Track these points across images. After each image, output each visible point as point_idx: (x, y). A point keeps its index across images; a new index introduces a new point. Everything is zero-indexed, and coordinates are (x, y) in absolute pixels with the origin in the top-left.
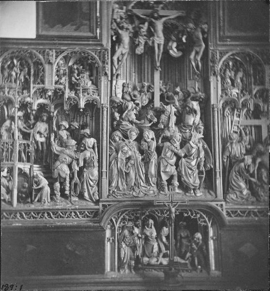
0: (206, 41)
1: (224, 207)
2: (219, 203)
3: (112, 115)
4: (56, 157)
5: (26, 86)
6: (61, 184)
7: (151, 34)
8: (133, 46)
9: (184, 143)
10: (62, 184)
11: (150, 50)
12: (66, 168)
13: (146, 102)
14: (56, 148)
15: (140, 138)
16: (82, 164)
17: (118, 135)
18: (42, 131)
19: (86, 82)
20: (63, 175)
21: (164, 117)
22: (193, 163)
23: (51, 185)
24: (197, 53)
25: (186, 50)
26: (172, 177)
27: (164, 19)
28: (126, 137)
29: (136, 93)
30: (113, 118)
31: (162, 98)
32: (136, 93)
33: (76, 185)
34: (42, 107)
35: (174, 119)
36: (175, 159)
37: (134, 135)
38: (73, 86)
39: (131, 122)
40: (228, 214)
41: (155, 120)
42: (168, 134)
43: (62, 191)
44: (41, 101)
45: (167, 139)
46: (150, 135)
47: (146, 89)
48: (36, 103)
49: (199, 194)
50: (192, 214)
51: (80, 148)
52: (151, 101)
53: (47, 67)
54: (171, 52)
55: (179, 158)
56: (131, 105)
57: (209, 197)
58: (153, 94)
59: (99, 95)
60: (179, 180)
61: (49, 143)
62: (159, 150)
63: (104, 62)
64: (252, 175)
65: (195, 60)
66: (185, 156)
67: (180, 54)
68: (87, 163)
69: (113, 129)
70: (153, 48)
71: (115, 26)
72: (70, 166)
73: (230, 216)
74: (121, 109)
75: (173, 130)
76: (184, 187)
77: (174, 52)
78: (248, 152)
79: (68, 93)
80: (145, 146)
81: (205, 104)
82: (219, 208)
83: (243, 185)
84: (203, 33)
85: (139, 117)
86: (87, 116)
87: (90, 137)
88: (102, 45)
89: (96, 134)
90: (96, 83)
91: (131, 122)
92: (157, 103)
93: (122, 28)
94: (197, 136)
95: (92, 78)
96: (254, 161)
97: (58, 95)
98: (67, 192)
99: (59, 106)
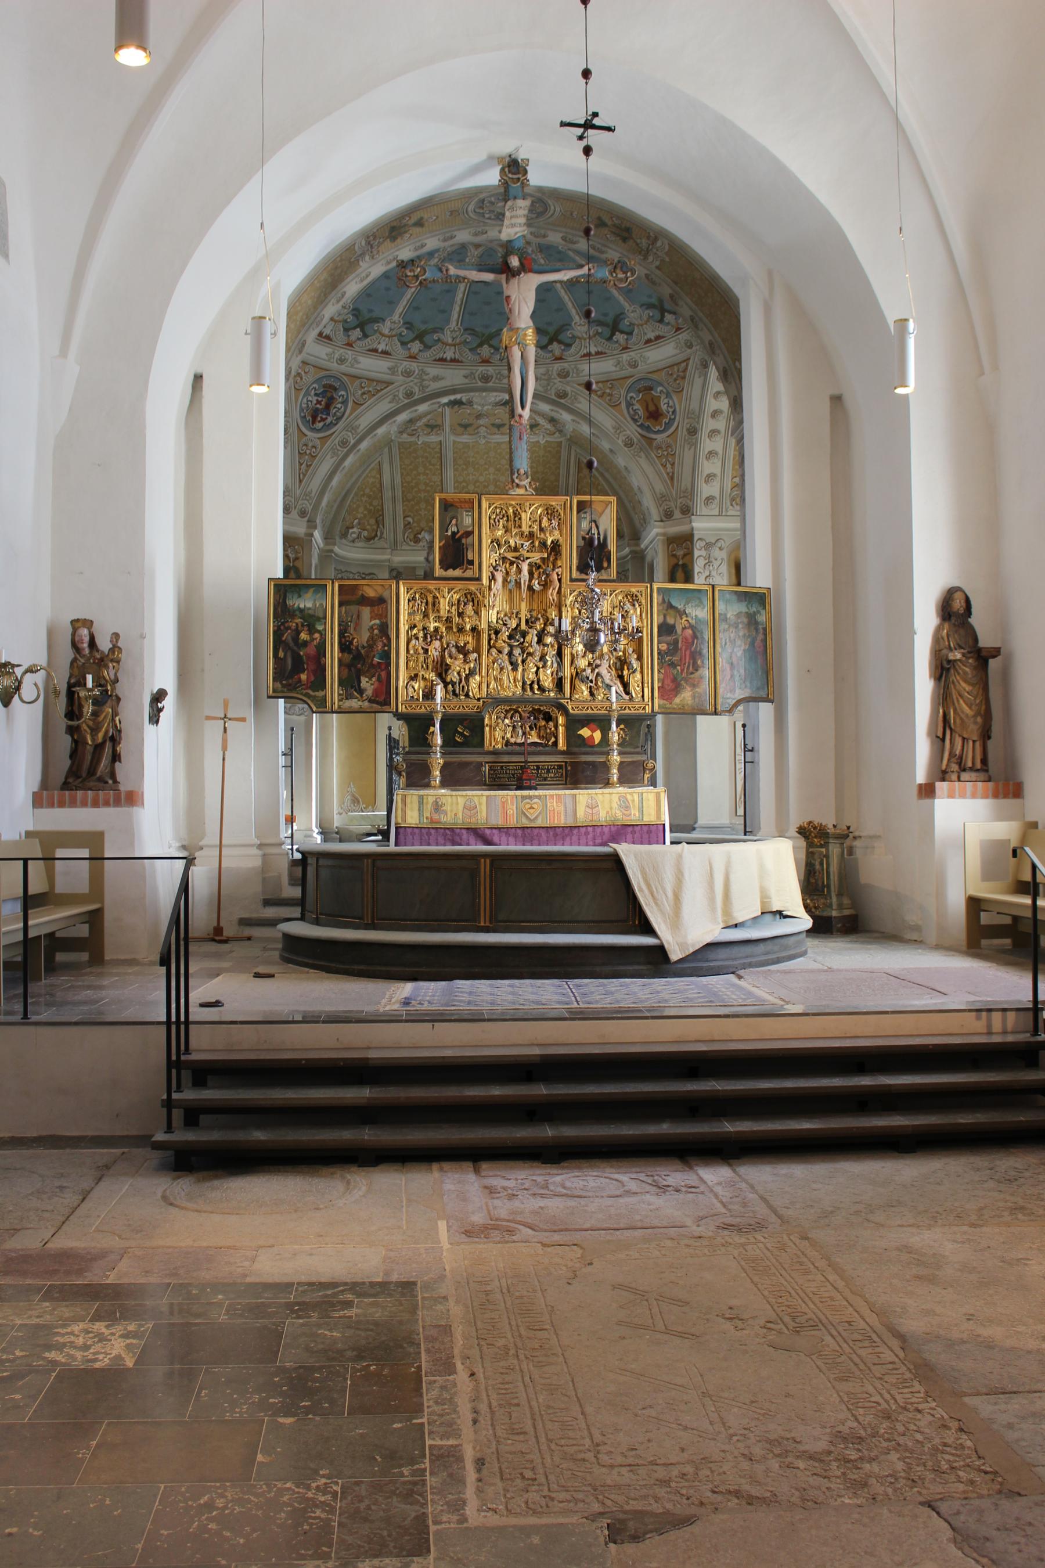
0: (560, 580)
3: (489, 635)
4: (448, 668)
5: (426, 615)
6: (453, 686)
8: (505, 581)
9: (542, 658)
11: (518, 584)
12: (455, 674)
13: (514, 626)
14: (448, 661)
15: (510, 654)
16: (467, 672)
17: (494, 651)
18: (437, 647)
19: (469, 610)
20: (454, 680)
21: (528, 638)
22: (549, 672)
23: (445, 687)
24: (554, 589)
25: (545, 585)
26: (533, 682)
27: (529, 561)
28: (500, 652)
29: (507, 618)
30: (490, 640)
31: (527, 621)
32: (507, 618)
33: (463, 687)
34: (436, 629)
35: (536, 639)
36: (535, 669)
37: (506, 650)
38: (460, 615)
39: (504, 642)
41: (522, 640)
44: (436, 624)
45: (530, 654)
46: (517, 652)
47: (514, 615)
48: (432, 626)
49: (552, 694)
51: (465, 661)
52: (518, 625)
53: (442, 600)
55: (538, 668)
56: (504, 628)
57: (559, 696)
58: (520, 619)
59: (480, 621)
60: (538, 684)
61: (443, 657)
62: (523, 661)
63: (483, 597)
64: (591, 681)
65: (552, 595)
66: (543, 667)
67: (542, 587)
68: (471, 673)
69: (490, 647)
70: (520, 583)
71: (491, 569)
72: (459, 673)
74: (497, 632)
75: (536, 649)
76: (542, 689)
77: (537, 587)
78: (590, 664)
79: (456, 619)
80: (514, 659)
83: (584, 688)
84: (558, 575)
85: (510, 637)
87: (473, 652)
89: (477, 650)
90: (477, 613)
91: (504, 642)
92: (523, 626)
96: (593, 671)
97: (449, 620)
98: (457, 692)
99: (449, 629)
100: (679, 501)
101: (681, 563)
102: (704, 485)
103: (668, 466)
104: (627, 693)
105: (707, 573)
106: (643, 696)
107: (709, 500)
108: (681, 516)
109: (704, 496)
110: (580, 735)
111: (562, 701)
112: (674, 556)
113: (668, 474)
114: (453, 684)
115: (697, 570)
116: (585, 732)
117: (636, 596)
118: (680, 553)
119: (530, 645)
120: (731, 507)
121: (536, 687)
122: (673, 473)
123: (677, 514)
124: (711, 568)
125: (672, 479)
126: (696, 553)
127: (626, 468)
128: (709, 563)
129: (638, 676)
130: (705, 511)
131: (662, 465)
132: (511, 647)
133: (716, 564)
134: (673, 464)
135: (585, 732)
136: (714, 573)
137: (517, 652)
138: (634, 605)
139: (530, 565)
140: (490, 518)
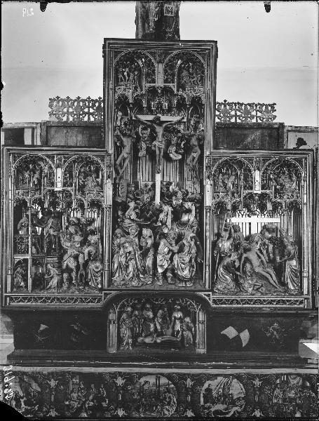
1: (211, 296)
2: (207, 293)
7: (153, 137)
9: (180, 238)
10: (70, 275)
16: (86, 258)
22: (187, 259)
27: (164, 125)
31: (162, 195)
33: (82, 275)
40: (214, 301)
42: (166, 231)
43: (70, 279)
50: (183, 302)
52: (153, 198)
54: (171, 155)
71: (118, 132)
72: (76, 257)
73: (216, 304)
74: (125, 207)
81: (200, 202)
82: (207, 298)
86: (94, 212)
88: (107, 152)
93: (125, 135)
94: (190, 234)
95: (97, 180)
104: (284, 284)
106: (301, 287)
110: (223, 334)
111: (202, 294)
114: (69, 270)
116: (231, 332)
117: (295, 167)
119: (164, 224)
121: (169, 274)
129: (294, 263)
132: (141, 227)
135: (231, 332)
137: (147, 232)
138: (291, 177)
139: (166, 129)
140: (117, 72)
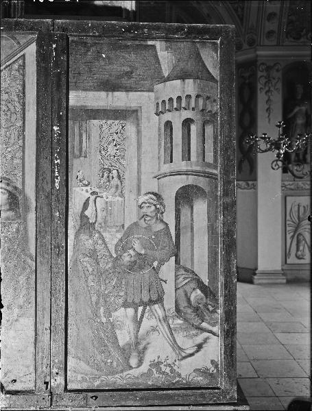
100: (247, 36)
101: (247, 81)
102: (267, 21)
103: (239, 9)
105: (267, 89)
107: (270, 33)
108: (248, 47)
109: (267, 30)
112: (243, 77)
113: (238, 16)
115: (259, 86)
118: (247, 75)
120: (286, 39)
122: (243, 15)
123: (245, 46)
124: (270, 85)
125: (242, 20)
126: (260, 74)
127: (208, 15)
128: (268, 81)
130: (267, 42)
131: (235, 10)
133: (274, 82)
134: (243, 9)
136: (272, 89)
